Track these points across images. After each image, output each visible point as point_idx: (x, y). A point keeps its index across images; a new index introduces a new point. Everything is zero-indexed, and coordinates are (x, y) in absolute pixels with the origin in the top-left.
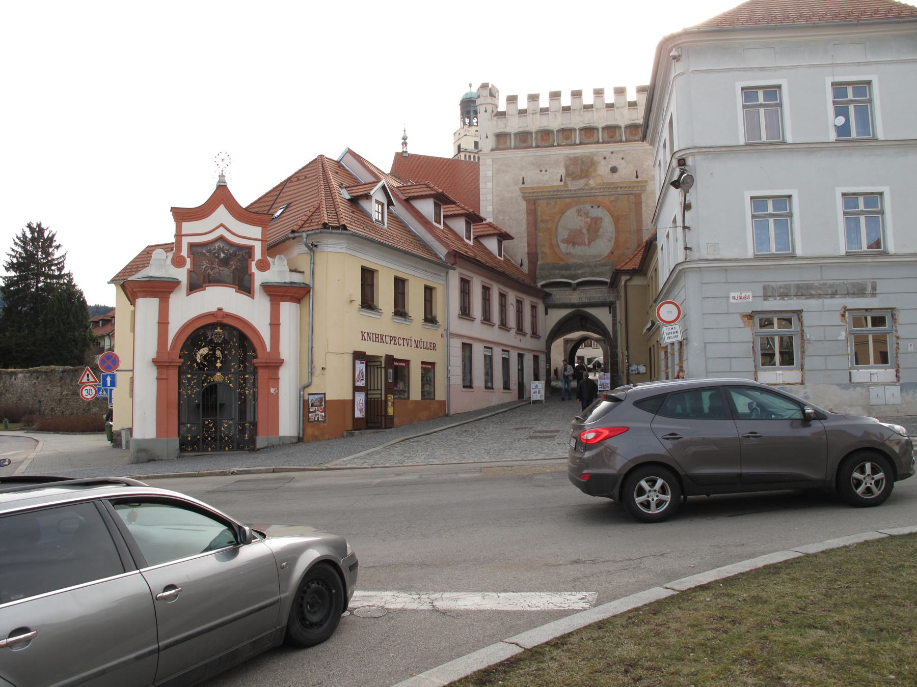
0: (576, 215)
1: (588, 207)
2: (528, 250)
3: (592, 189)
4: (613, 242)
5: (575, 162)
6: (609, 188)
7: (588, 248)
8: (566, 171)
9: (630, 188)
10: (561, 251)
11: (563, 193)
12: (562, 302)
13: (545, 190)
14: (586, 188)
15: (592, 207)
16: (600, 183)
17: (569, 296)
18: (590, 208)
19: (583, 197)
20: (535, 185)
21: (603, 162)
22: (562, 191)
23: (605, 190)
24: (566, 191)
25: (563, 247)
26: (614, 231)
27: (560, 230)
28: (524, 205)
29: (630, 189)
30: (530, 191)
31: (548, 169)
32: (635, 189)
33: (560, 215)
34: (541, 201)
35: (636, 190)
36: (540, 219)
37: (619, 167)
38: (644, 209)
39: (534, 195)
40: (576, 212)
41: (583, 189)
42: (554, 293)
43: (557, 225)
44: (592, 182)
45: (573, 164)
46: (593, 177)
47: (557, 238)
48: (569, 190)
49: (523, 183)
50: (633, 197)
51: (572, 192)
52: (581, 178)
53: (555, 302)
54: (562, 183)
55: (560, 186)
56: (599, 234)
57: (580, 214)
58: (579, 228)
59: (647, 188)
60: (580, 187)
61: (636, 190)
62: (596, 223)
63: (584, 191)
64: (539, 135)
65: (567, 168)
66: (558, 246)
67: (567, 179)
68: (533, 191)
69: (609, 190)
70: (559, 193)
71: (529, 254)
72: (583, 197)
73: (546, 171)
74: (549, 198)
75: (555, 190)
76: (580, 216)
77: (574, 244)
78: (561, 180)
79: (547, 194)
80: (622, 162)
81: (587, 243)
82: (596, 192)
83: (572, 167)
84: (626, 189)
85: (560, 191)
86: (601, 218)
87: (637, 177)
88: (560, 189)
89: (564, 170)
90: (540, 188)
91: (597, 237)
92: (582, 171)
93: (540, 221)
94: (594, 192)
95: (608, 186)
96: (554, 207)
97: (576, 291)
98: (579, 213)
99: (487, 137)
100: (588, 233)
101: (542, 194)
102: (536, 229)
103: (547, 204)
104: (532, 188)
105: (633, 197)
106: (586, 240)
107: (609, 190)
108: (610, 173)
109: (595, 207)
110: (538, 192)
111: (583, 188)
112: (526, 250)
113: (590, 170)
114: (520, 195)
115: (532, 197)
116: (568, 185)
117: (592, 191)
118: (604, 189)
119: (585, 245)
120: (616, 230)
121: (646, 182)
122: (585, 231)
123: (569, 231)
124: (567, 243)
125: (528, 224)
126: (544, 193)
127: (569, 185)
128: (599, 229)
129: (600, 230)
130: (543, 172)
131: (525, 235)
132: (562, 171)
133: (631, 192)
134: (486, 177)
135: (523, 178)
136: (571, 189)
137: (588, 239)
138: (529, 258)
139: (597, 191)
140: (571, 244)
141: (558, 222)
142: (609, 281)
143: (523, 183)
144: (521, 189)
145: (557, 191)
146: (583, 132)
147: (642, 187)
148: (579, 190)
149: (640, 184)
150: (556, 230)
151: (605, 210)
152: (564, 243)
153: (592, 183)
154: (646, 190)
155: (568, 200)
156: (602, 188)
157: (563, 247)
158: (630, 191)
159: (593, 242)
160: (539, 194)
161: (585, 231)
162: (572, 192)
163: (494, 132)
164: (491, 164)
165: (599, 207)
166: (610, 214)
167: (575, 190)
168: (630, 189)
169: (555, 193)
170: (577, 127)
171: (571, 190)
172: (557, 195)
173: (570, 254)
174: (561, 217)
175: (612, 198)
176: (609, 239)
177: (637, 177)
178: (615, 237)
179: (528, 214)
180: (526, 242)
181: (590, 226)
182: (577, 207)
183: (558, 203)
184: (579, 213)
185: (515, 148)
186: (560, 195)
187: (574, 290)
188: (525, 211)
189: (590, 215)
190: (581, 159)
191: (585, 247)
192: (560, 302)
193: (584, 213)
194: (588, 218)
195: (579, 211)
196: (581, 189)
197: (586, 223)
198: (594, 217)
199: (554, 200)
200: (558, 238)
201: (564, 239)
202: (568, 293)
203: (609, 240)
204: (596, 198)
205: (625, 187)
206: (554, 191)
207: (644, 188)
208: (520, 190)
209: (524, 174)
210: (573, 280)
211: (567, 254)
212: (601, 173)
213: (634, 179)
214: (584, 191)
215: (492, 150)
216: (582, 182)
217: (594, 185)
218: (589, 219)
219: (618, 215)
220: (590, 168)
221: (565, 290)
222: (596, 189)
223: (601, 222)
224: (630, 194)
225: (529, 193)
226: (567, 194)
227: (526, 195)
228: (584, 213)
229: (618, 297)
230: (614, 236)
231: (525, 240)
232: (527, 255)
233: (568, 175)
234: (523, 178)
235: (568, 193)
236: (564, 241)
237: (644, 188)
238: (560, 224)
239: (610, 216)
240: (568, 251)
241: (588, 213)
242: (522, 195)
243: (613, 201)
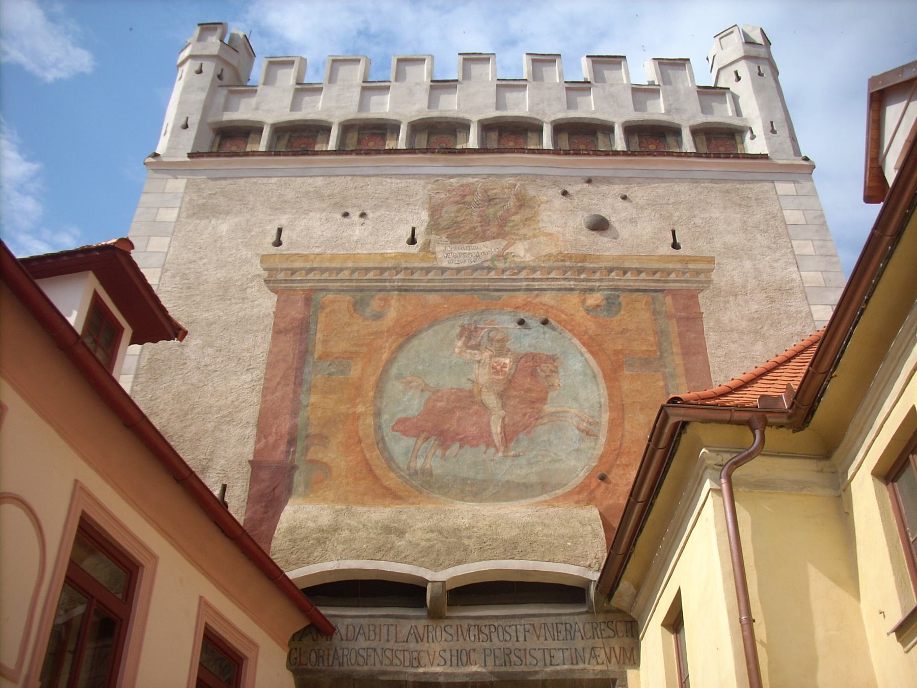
0: (460, 343)
1: (506, 323)
2: (257, 453)
3: (522, 269)
4: (603, 439)
5: (464, 196)
6: (581, 270)
7: (500, 454)
8: (432, 215)
9: (655, 273)
10: (390, 460)
11: (415, 276)
12: (378, 667)
13: (350, 264)
14: (501, 265)
15: (521, 322)
16: (549, 256)
17: (412, 645)
18: (513, 326)
19: (488, 290)
20: (317, 251)
21: (559, 202)
22: (413, 271)
23: (568, 275)
24: (428, 270)
25: (400, 446)
26: (604, 400)
27: (394, 387)
28: (267, 303)
29: (657, 276)
30: (296, 265)
31: (368, 212)
32: (673, 276)
33: (401, 340)
34: (331, 296)
35: (674, 281)
36: (319, 349)
37: (613, 219)
38: (711, 339)
39: (311, 276)
40: (460, 336)
41: (489, 269)
42: (343, 631)
43: (385, 371)
44: (521, 252)
45: (457, 203)
46: (525, 237)
47: (378, 414)
48: (434, 268)
49: (278, 243)
50: (669, 300)
51: (447, 275)
52: (483, 237)
53: (346, 668)
54: (414, 249)
55: (404, 255)
56: (548, 408)
57: (472, 342)
58: (468, 386)
59: (714, 276)
60: (479, 262)
61: (674, 281)
62: (533, 374)
63: (492, 275)
64: (353, 138)
65: (435, 211)
66: (381, 442)
67: (433, 237)
68: (308, 266)
69: (583, 276)
70: (400, 276)
71: (256, 465)
72: (488, 290)
73: (363, 215)
74: (362, 290)
75: (385, 265)
76: (477, 347)
77: (444, 438)
78: (412, 241)
79: (356, 276)
80: (626, 204)
81: (497, 439)
82: (533, 280)
83: (454, 208)
84: (643, 276)
85: (406, 269)
86: (553, 359)
87: (675, 246)
88: (404, 266)
89: (425, 216)
90: (333, 257)
91: (538, 416)
92: (485, 221)
93: (320, 358)
94: (526, 279)
95: (579, 265)
96: (378, 316)
97: (447, 622)
98: (469, 338)
99: (186, 126)
100: (503, 406)
101: (340, 276)
102: (299, 383)
103: (355, 304)
104: (305, 257)
105: (669, 300)
106: (496, 429)
107: (583, 276)
108: (587, 232)
109: (534, 323)
110: (323, 270)
111: (486, 264)
112: (248, 451)
113: (516, 218)
114: (259, 275)
115: (301, 281)
116: (434, 253)
117: (523, 275)
118: (565, 272)
119: (489, 443)
120: (611, 396)
121: (711, 260)
122: (491, 400)
123: (427, 394)
124: (417, 436)
125: (271, 366)
126: (346, 273)
127: (439, 256)
128: (547, 392)
129: (552, 394)
130: (355, 217)
131: (255, 398)
132: (421, 219)
133: (660, 285)
134: (155, 221)
135: (280, 231)
136: (445, 264)
137: (504, 427)
138: (254, 479)
139: (538, 275)
140: (433, 438)
141: (391, 361)
142: (595, 576)
143: (278, 243)
144: (264, 258)
145: (395, 268)
146: (494, 136)
147: (698, 273)
148: (475, 269)
149: (691, 266)
150: (379, 388)
151: (569, 335)
152: (405, 433)
153: (522, 253)
154: (709, 282)
155: (433, 298)
156: (558, 268)
157: (400, 446)
158: (658, 281)
159: (521, 436)
160: (326, 276)
161: (491, 400)
162: (447, 275)
163: (211, 119)
164: (182, 190)
165: (545, 322)
166: (584, 344)
167: (459, 270)
168: (657, 276)
169: (386, 275)
170: (474, 118)
171: (443, 270)
172: (390, 281)
173: (427, 473)
174: (400, 347)
175: (593, 299)
176: (584, 425)
177: (675, 246)
178: (612, 421)
179: (278, 332)
180: (253, 421)
181: (510, 382)
182: (466, 320)
183: (393, 302)
184: (469, 338)
185: (267, 153)
186: (403, 280)
187: (435, 615)
188: (270, 321)
189: (509, 345)
190: (486, 191)
191: (492, 450)
192: (366, 668)
193: (491, 340)
194: (505, 356)
195: (469, 334)
196: (483, 268)
197: (497, 372)
198: (526, 355)
199: (381, 294)
200: (385, 416)
201: (406, 419)
202: (405, 627)
203: (587, 433)
204: (537, 296)
205: (639, 271)
206: (383, 270)
207: (702, 277)
208: (261, 262)
209: (283, 220)
210: (437, 565)
211: (416, 472)
212: (553, 229)
213: (667, 250)
214: (492, 275)
215: (190, 155)
216: (487, 249)
217: (529, 258)
218: (507, 361)
219: (617, 352)
220: (516, 213)
221: (398, 617)
222: (534, 270)
223: (555, 371)
224: (656, 291)
225: (294, 271)
226: (429, 281)
227: (281, 276)
228: (491, 340)
229: (632, 657)
230: (605, 418)
231: (250, 413)
232: (248, 468)
233: (434, 226)
234: (280, 231)
235: (431, 276)
236: (404, 426)
237: (702, 277)
238: (394, 371)
239: (588, 356)
240: (419, 463)
241: (503, 341)
242: (265, 274)
243: (598, 306)
